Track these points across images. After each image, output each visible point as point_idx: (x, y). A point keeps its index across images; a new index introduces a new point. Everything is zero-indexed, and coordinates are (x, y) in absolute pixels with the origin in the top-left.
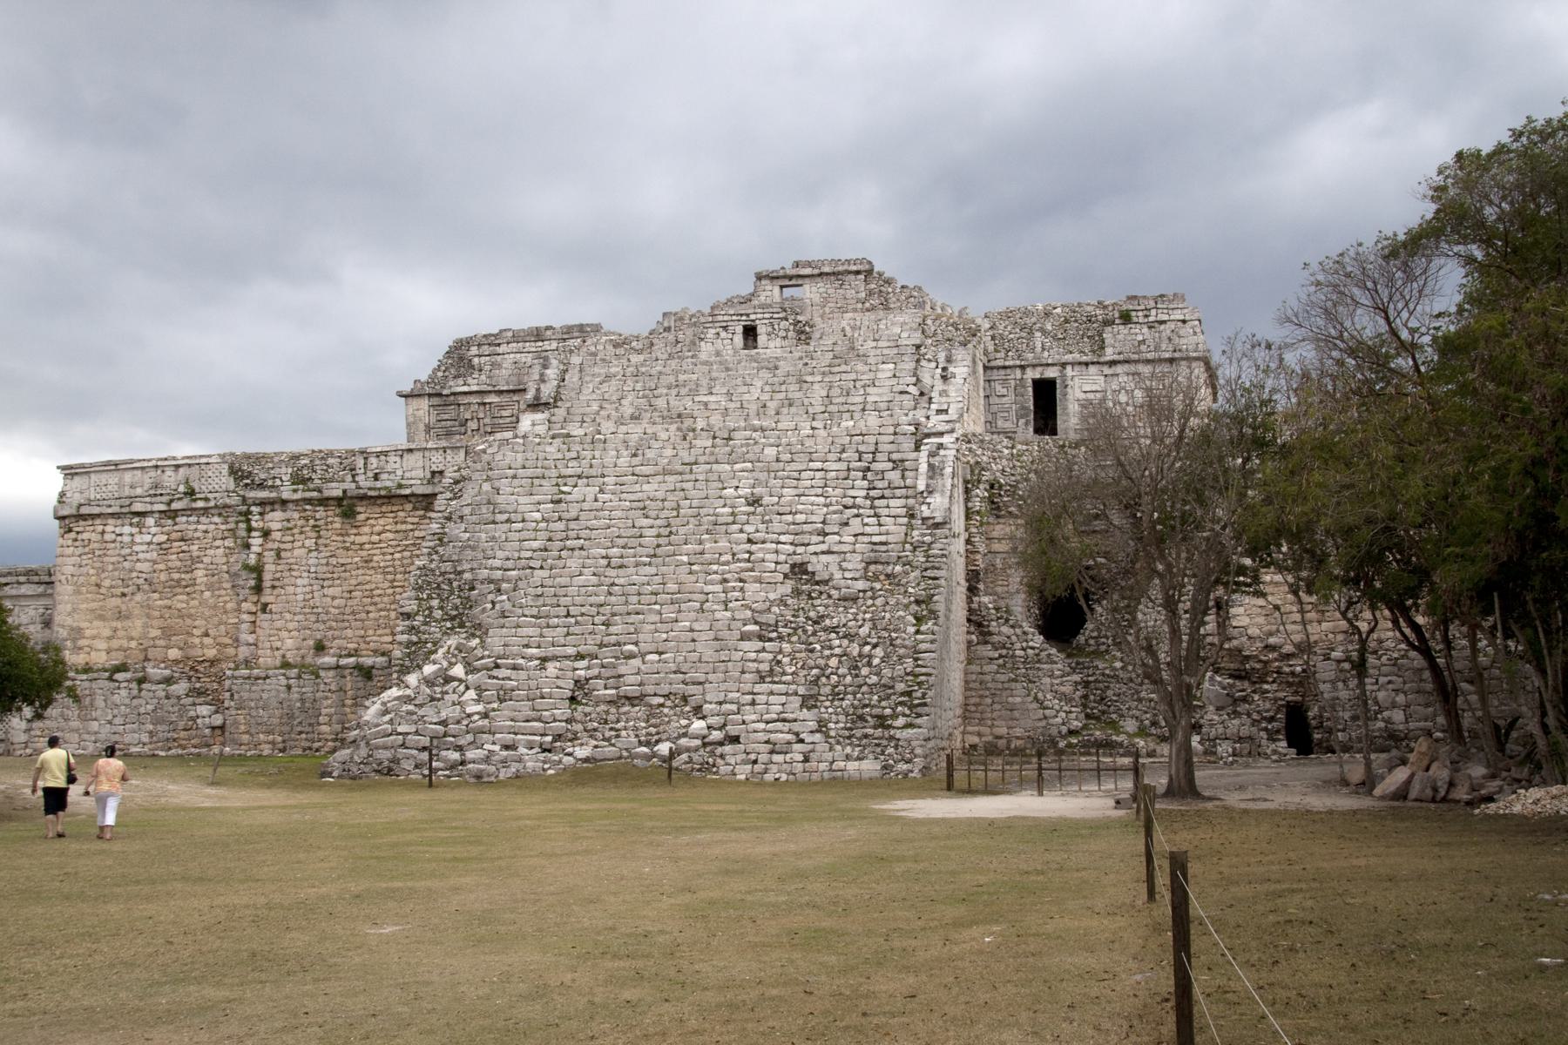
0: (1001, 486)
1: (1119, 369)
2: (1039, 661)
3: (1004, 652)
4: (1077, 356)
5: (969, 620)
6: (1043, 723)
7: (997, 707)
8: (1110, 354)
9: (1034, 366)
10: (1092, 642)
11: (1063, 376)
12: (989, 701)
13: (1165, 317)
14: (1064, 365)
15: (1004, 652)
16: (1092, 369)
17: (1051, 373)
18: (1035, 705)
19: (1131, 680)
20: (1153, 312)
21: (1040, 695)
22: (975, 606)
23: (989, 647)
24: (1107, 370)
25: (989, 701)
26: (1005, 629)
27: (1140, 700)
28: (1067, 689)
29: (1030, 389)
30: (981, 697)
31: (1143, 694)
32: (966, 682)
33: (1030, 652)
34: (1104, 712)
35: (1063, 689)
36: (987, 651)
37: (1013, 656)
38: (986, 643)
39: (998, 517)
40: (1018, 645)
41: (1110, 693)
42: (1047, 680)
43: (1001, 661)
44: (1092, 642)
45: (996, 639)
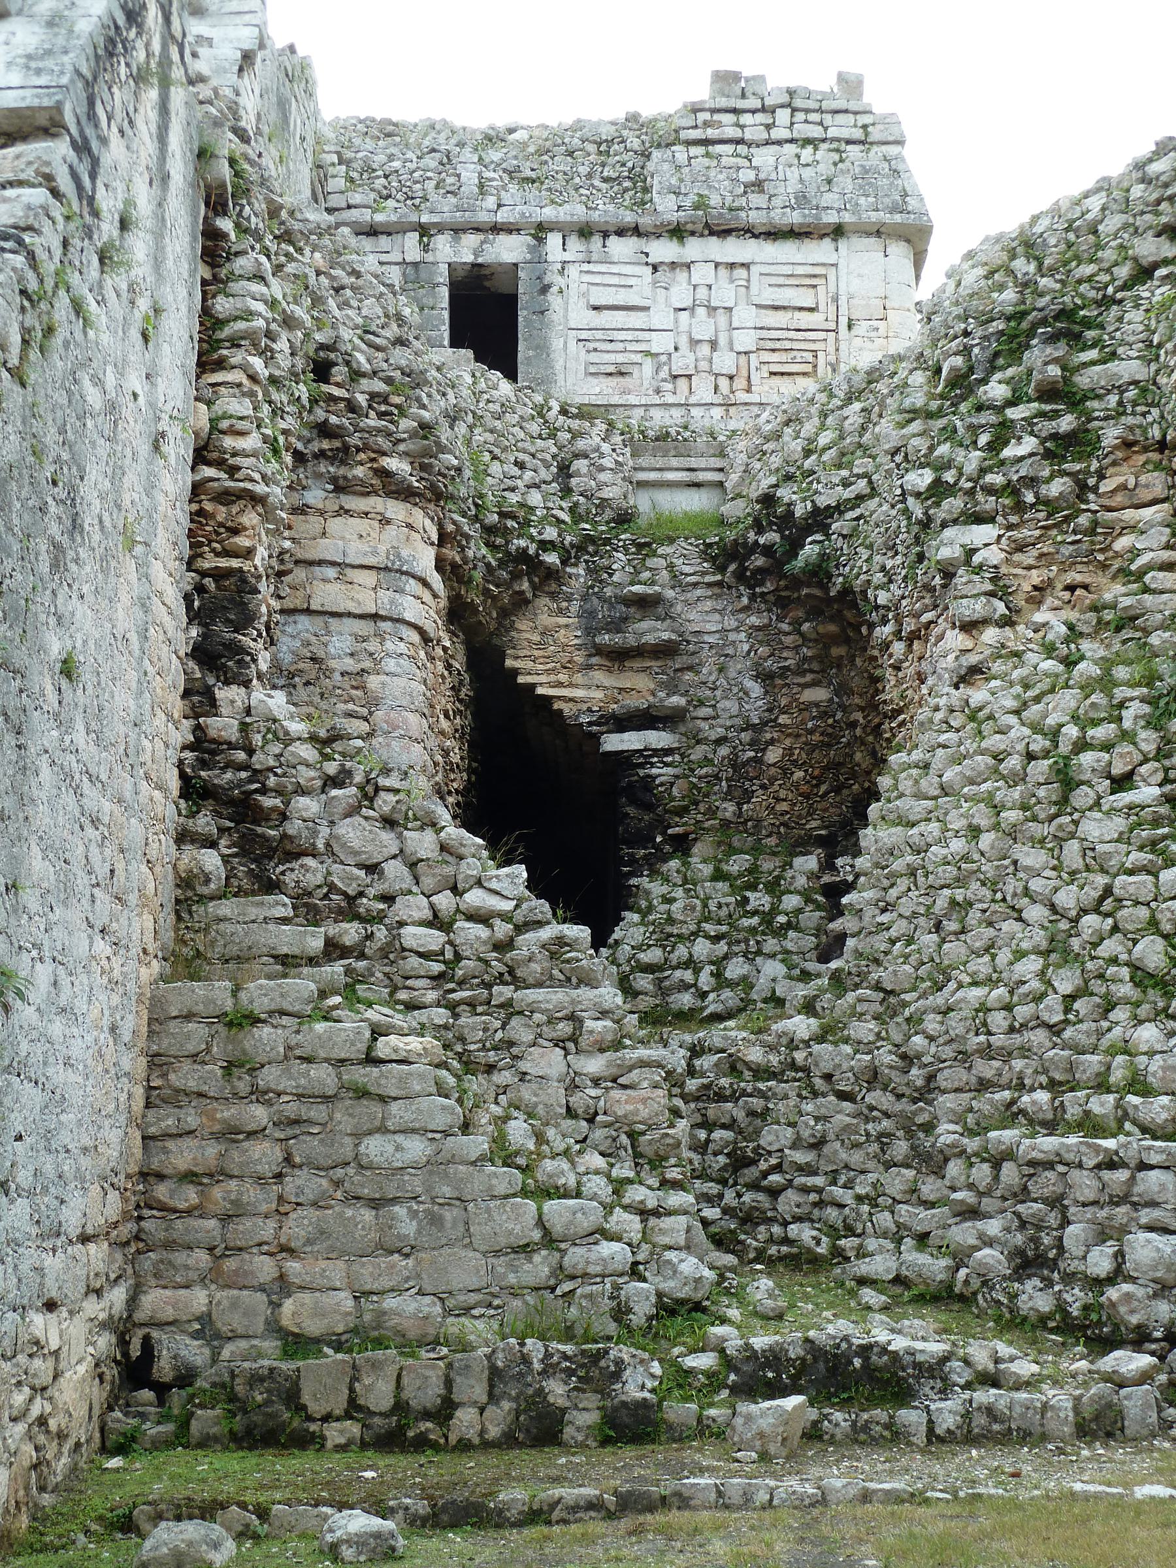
0: (356, 375)
1: (694, 248)
2: (511, 976)
3: (351, 932)
4: (573, 211)
5: (193, 791)
6: (539, 1267)
7: (303, 1183)
8: (666, 207)
9: (458, 230)
10: (643, 982)
11: (538, 259)
12: (264, 1154)
13: (816, 132)
14: (541, 230)
15: (351, 932)
16: (620, 247)
17: (507, 250)
18: (505, 1178)
19: (873, 1077)
20: (783, 116)
21: (518, 1131)
22: (224, 726)
23: (281, 905)
24: (663, 250)
25: (264, 1154)
26: (357, 833)
27: (933, 1162)
28: (644, 1101)
29: (444, 292)
30: (231, 1134)
31: (947, 1134)
32: (157, 1062)
33: (471, 933)
34: (749, 1219)
35: (621, 1102)
36: (266, 923)
37: (394, 951)
38: (272, 886)
39: (341, 487)
40: (414, 907)
41: (774, 1136)
42: (548, 1062)
43: (336, 970)
44: (643, 982)
45: (310, 873)
